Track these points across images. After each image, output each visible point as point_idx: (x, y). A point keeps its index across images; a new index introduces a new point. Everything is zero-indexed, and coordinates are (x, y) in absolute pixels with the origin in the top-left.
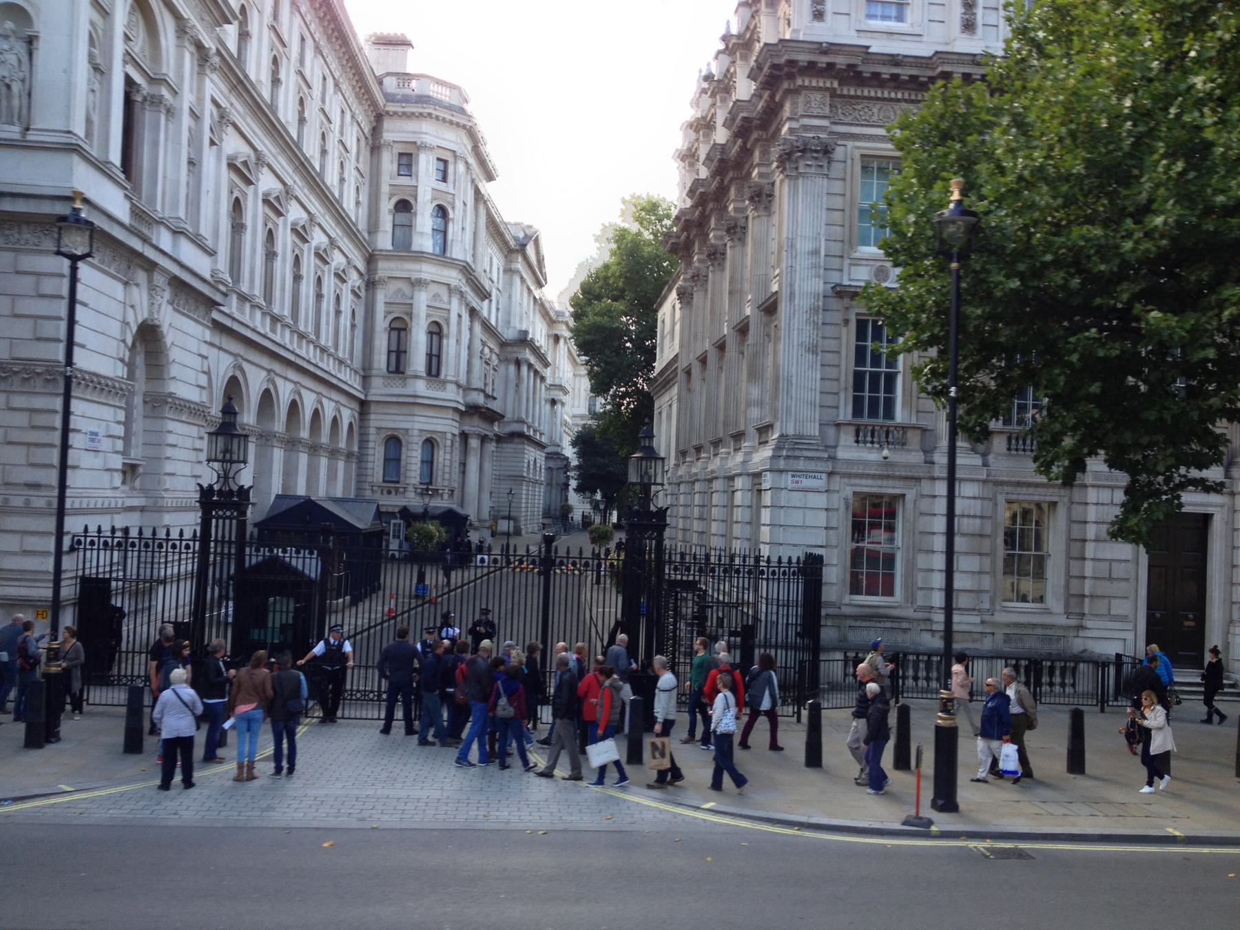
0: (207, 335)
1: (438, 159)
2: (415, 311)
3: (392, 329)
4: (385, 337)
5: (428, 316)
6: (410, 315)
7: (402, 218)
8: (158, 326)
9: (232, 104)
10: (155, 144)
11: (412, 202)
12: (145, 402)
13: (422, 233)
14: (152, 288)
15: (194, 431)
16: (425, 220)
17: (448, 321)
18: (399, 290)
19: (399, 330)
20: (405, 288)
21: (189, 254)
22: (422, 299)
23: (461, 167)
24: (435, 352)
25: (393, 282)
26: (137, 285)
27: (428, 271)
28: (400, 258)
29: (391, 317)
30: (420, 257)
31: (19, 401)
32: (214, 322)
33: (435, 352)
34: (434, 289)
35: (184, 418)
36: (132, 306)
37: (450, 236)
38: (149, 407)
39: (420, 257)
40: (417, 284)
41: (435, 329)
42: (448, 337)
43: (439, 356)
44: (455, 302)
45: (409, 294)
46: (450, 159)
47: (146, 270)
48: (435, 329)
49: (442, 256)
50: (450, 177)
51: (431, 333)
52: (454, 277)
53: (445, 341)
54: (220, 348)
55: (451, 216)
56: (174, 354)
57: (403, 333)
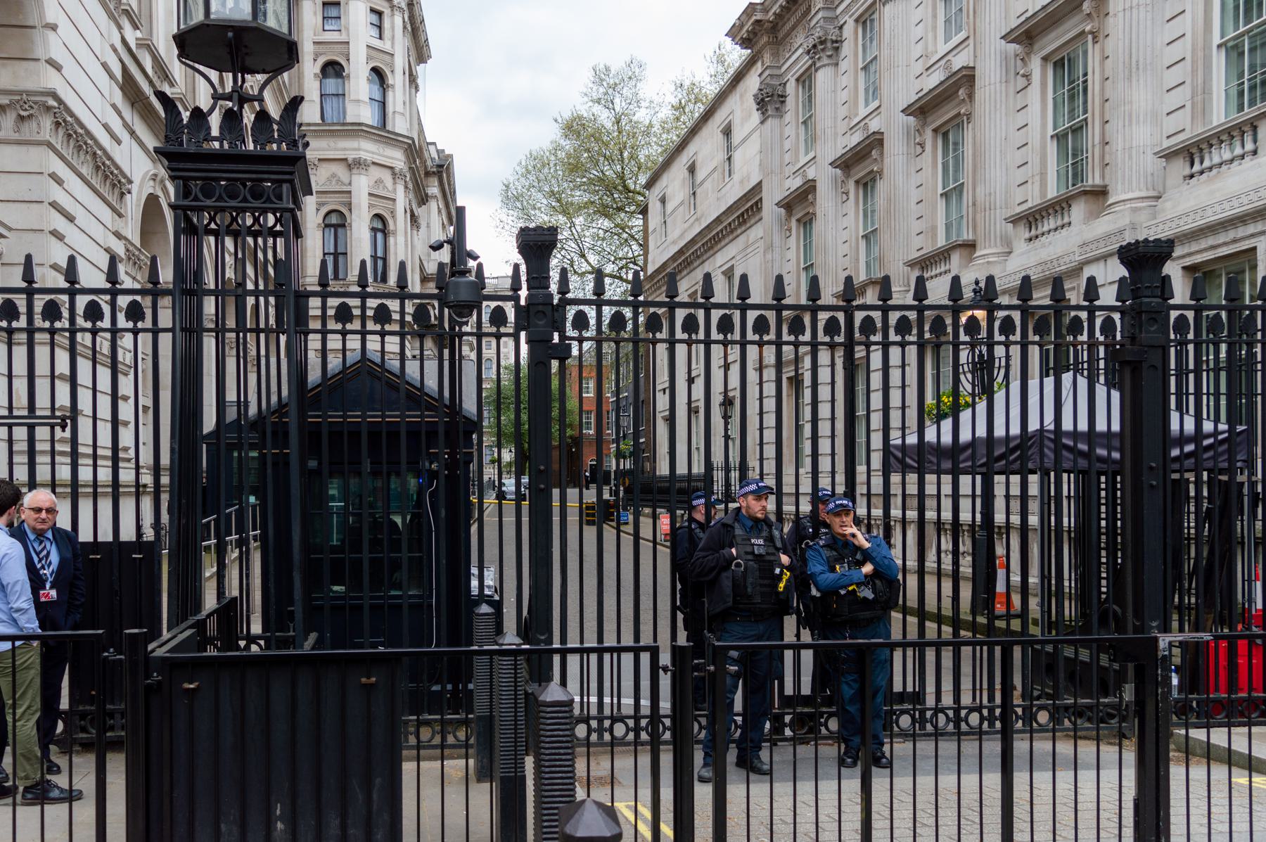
1: (373, 10)
2: (354, 201)
3: (327, 226)
4: (319, 234)
5: (371, 206)
6: (349, 206)
7: (332, 84)
11: (344, 63)
13: (358, 101)
16: (360, 85)
17: (393, 213)
18: (334, 175)
19: (336, 226)
20: (340, 170)
22: (362, 185)
23: (398, 20)
24: (380, 254)
25: (325, 165)
27: (367, 149)
28: (332, 134)
29: (324, 210)
30: (357, 130)
33: (380, 254)
34: (376, 173)
37: (390, 109)
39: (357, 130)
40: (355, 165)
41: (380, 226)
42: (394, 233)
43: (385, 260)
44: (400, 189)
45: (347, 181)
46: (387, 11)
48: (380, 226)
49: (381, 131)
50: (387, 33)
51: (374, 230)
52: (397, 158)
53: (391, 240)
55: (390, 82)
57: (340, 230)
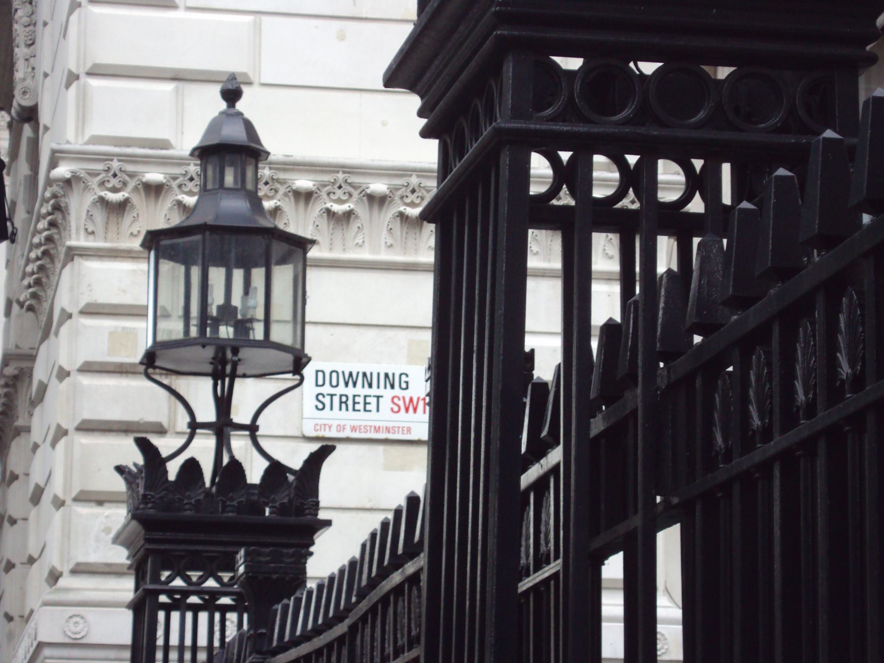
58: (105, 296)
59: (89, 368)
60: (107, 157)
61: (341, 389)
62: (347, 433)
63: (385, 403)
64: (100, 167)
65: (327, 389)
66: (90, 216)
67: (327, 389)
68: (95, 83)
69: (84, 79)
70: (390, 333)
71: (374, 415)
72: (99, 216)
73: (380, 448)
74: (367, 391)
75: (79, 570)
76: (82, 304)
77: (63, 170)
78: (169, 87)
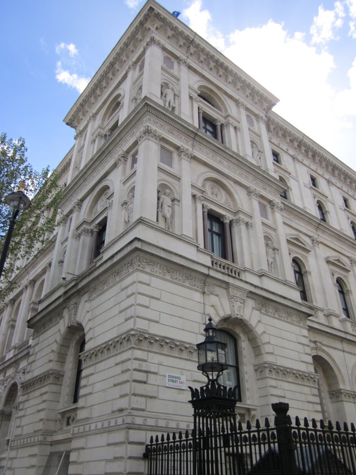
0: (305, 332)
8: (241, 320)
9: (318, 235)
10: (241, 238)
12: (256, 370)
14: (231, 298)
15: (307, 390)
21: (268, 284)
26: (217, 296)
31: (119, 358)
32: (309, 326)
35: (290, 380)
36: (213, 306)
38: (258, 373)
47: (226, 289)
54: (344, 351)
56: (265, 338)
58: (138, 357)
59: (135, 370)
60: (140, 332)
61: (172, 379)
62: (173, 387)
63: (178, 382)
64: (138, 333)
65: (170, 378)
66: (136, 342)
67: (170, 378)
68: (137, 319)
69: (135, 317)
70: (178, 369)
71: (176, 384)
72: (137, 342)
73: (177, 390)
74: (175, 379)
75: (133, 409)
76: (134, 357)
77: (133, 332)
78: (148, 321)
